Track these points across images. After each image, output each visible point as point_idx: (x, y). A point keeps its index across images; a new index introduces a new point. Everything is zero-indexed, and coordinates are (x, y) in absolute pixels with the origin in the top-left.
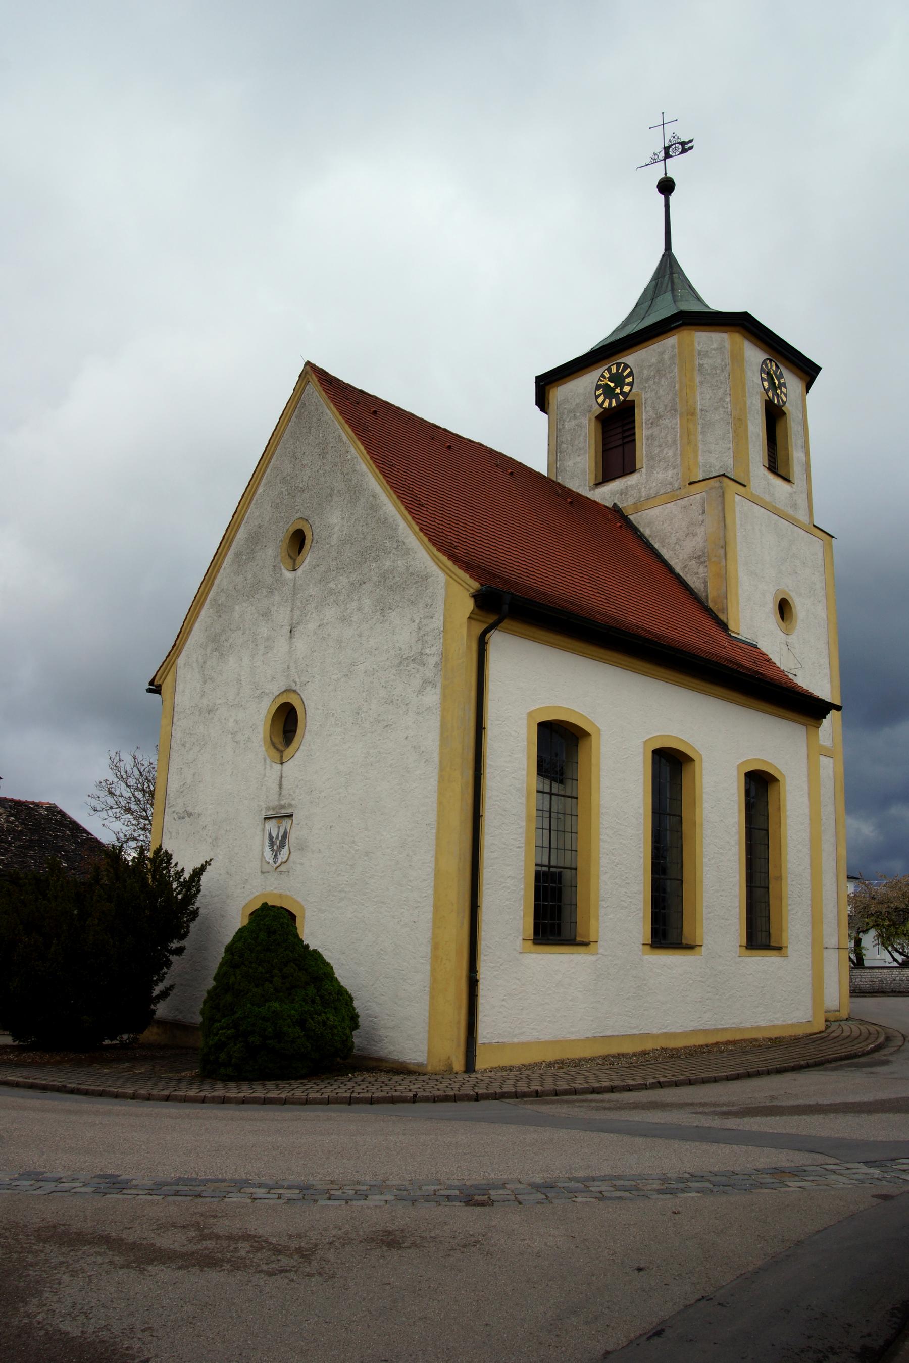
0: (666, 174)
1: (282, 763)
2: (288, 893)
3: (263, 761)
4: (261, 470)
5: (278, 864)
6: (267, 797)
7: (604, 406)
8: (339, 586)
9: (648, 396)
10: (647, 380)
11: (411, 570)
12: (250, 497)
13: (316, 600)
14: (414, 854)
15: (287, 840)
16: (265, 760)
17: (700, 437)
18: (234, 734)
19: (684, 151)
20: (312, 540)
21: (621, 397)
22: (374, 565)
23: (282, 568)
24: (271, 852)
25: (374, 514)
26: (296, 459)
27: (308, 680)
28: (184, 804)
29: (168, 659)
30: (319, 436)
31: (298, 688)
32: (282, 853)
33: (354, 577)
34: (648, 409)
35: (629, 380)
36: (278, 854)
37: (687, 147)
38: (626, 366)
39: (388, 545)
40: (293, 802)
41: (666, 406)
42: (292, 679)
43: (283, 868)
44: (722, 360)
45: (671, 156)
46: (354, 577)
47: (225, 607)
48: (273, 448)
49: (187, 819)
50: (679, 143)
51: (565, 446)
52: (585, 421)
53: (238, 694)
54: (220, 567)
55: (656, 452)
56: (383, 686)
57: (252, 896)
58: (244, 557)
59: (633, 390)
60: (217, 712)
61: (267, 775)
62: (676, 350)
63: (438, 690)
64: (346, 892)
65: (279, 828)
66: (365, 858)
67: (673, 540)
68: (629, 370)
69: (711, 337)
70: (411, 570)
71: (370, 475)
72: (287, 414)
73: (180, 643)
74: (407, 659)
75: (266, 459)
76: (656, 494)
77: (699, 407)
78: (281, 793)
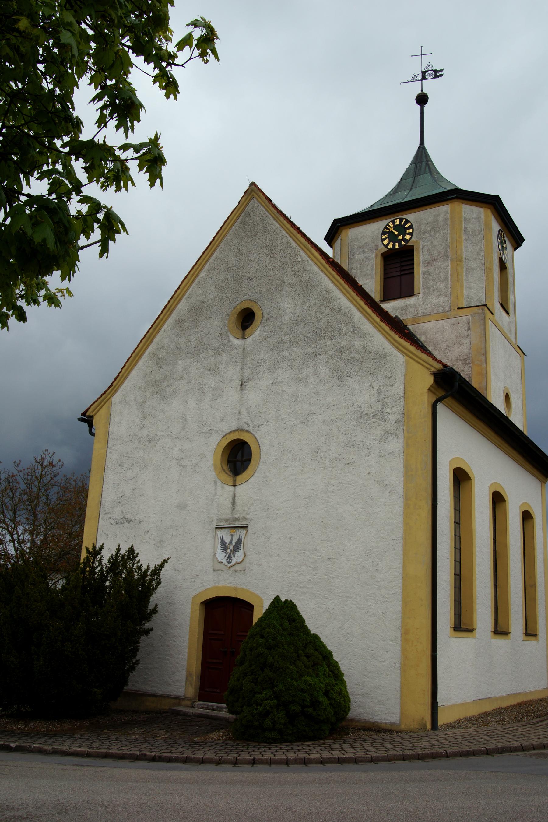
0: (422, 90)
1: (235, 486)
2: (244, 587)
3: (213, 482)
4: (204, 259)
5: (232, 564)
6: (218, 511)
7: (389, 247)
8: (293, 355)
9: (425, 244)
10: (425, 233)
11: (368, 349)
12: (193, 278)
13: (267, 363)
14: (380, 561)
15: (242, 546)
16: (215, 483)
17: (465, 277)
18: (179, 461)
19: (436, 77)
20: (262, 318)
21: (403, 242)
22: (330, 342)
23: (230, 335)
24: (224, 555)
25: (328, 305)
26: (242, 255)
27: (261, 424)
28: (122, 512)
29: (103, 397)
30: (266, 240)
31: (251, 429)
32: (236, 555)
33: (308, 349)
34: (424, 253)
35: (410, 231)
36: (232, 556)
37: (439, 74)
38: (407, 221)
39: (344, 329)
40: (248, 517)
41: (439, 253)
42: (243, 421)
43: (237, 567)
44: (479, 226)
45: (427, 79)
46: (308, 349)
47: (167, 360)
48: (217, 243)
49: (126, 524)
50: (432, 70)
51: (355, 271)
52: (372, 256)
53: (184, 429)
54: (160, 329)
55: (431, 284)
56: (342, 433)
57: (204, 589)
58: (187, 324)
59: (413, 239)
60: (160, 441)
61: (218, 494)
62: (449, 215)
63: (401, 440)
64: (308, 588)
65: (232, 536)
66: (329, 563)
67: (444, 345)
68: (409, 224)
69: (472, 209)
70: (368, 349)
71: (322, 275)
72: (232, 219)
73: (116, 385)
74: (367, 414)
75: (210, 251)
76: (430, 313)
77: (464, 257)
78: (234, 509)
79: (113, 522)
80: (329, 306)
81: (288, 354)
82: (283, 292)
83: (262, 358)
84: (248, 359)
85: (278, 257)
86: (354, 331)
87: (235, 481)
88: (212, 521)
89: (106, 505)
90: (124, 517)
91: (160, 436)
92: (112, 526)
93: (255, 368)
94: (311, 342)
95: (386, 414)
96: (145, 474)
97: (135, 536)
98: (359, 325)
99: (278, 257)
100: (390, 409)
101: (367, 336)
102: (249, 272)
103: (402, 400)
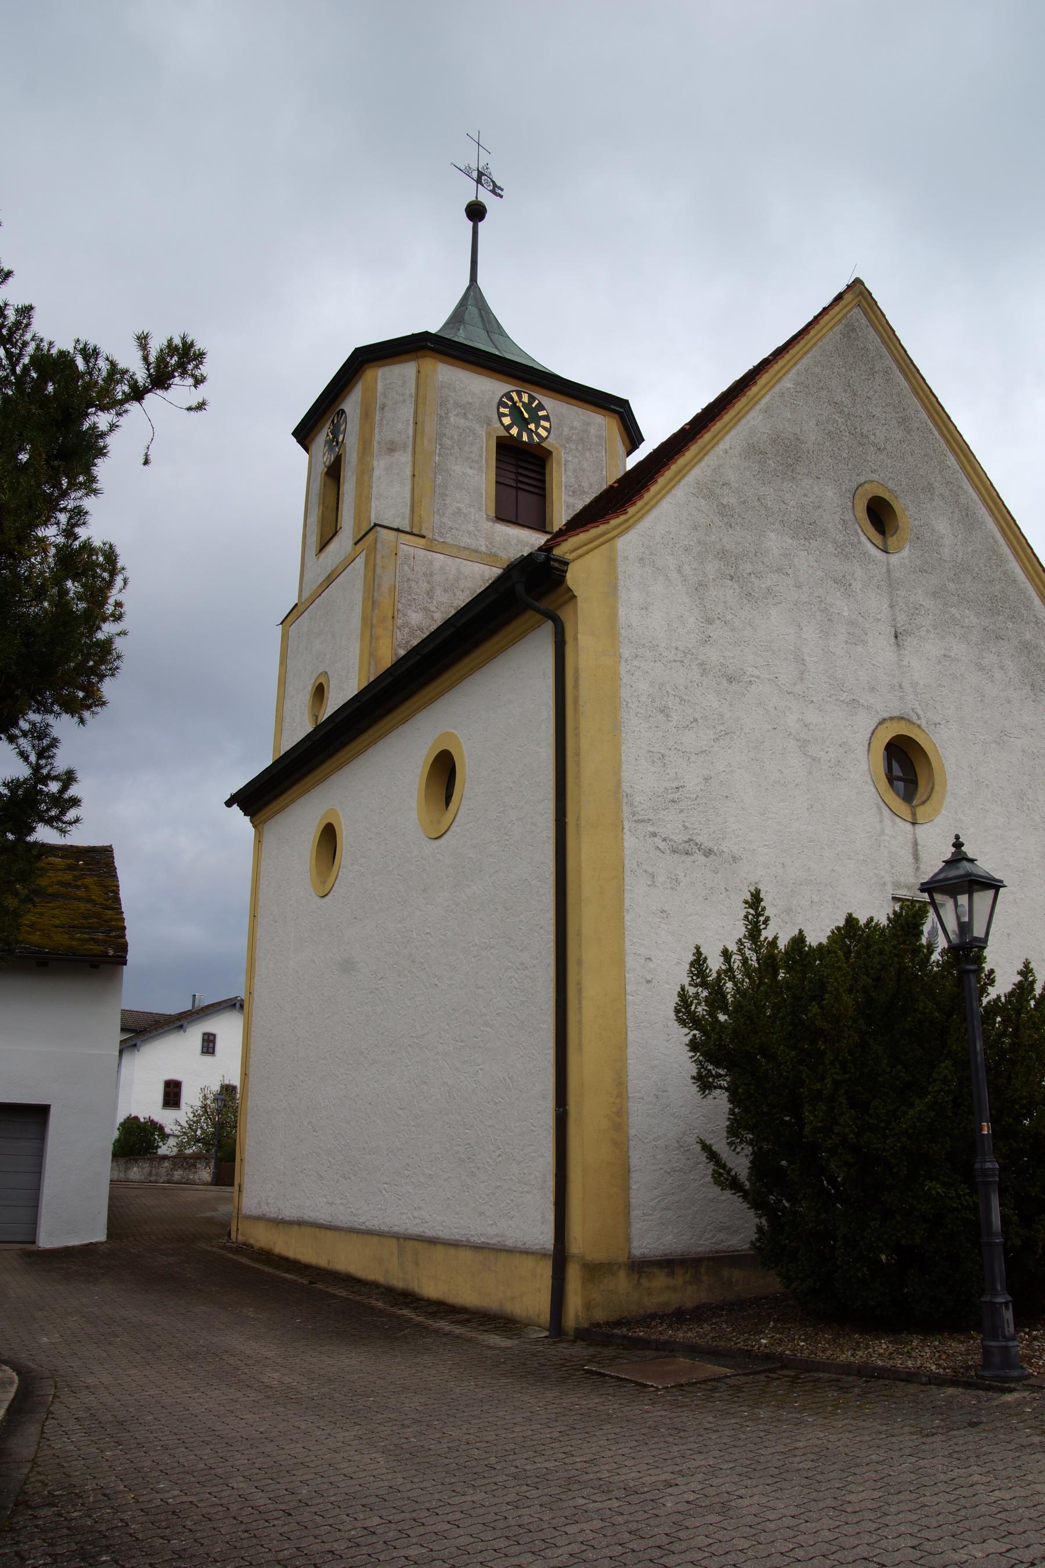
1: (914, 824)
3: (875, 808)
6: (892, 867)
49: (700, 858)
60: (753, 687)
61: (887, 831)
78: (918, 869)
79: (662, 845)
89: (637, 799)
90: (690, 840)
91: (753, 676)
92: (661, 854)
96: (730, 751)
97: (727, 890)
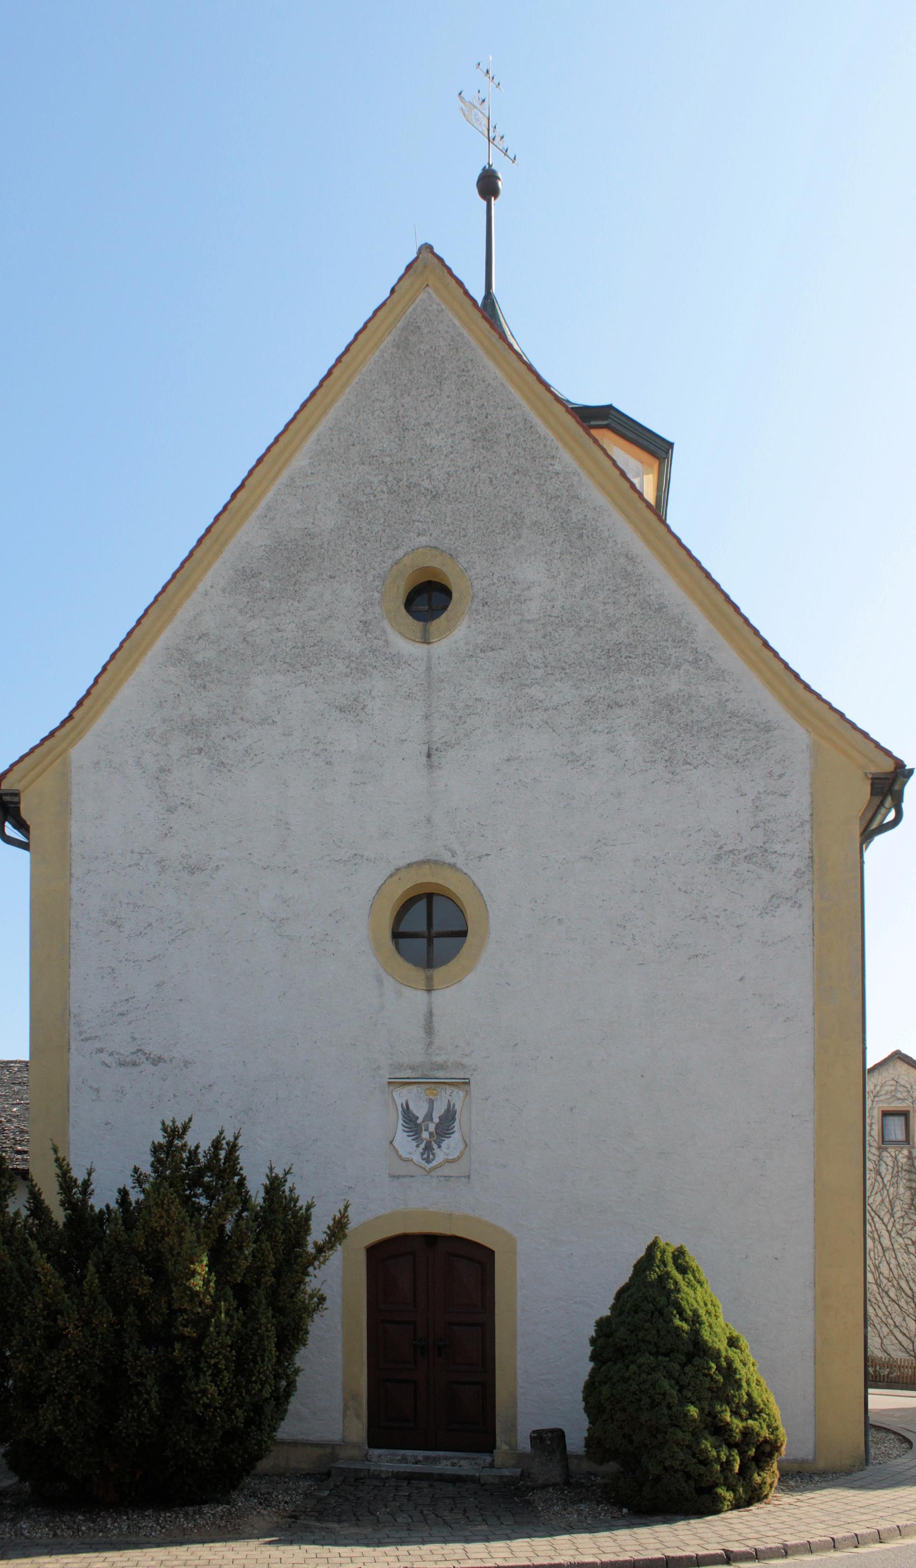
5: (434, 1163)
15: (456, 1124)
16: (380, 982)
22: (642, 679)
36: (435, 1146)
40: (466, 1061)
43: (447, 1170)
65: (431, 1102)
78: (430, 1044)
80: (635, 595)
81: (542, 696)
82: (522, 542)
83: (477, 696)
84: (440, 694)
85: (504, 452)
86: (696, 660)
87: (429, 980)
88: (379, 1068)
93: (461, 717)
94: (597, 674)
95: (774, 856)
98: (707, 649)
99: (504, 452)
100: (782, 845)
101: (727, 678)
102: (429, 477)
103: (807, 827)
